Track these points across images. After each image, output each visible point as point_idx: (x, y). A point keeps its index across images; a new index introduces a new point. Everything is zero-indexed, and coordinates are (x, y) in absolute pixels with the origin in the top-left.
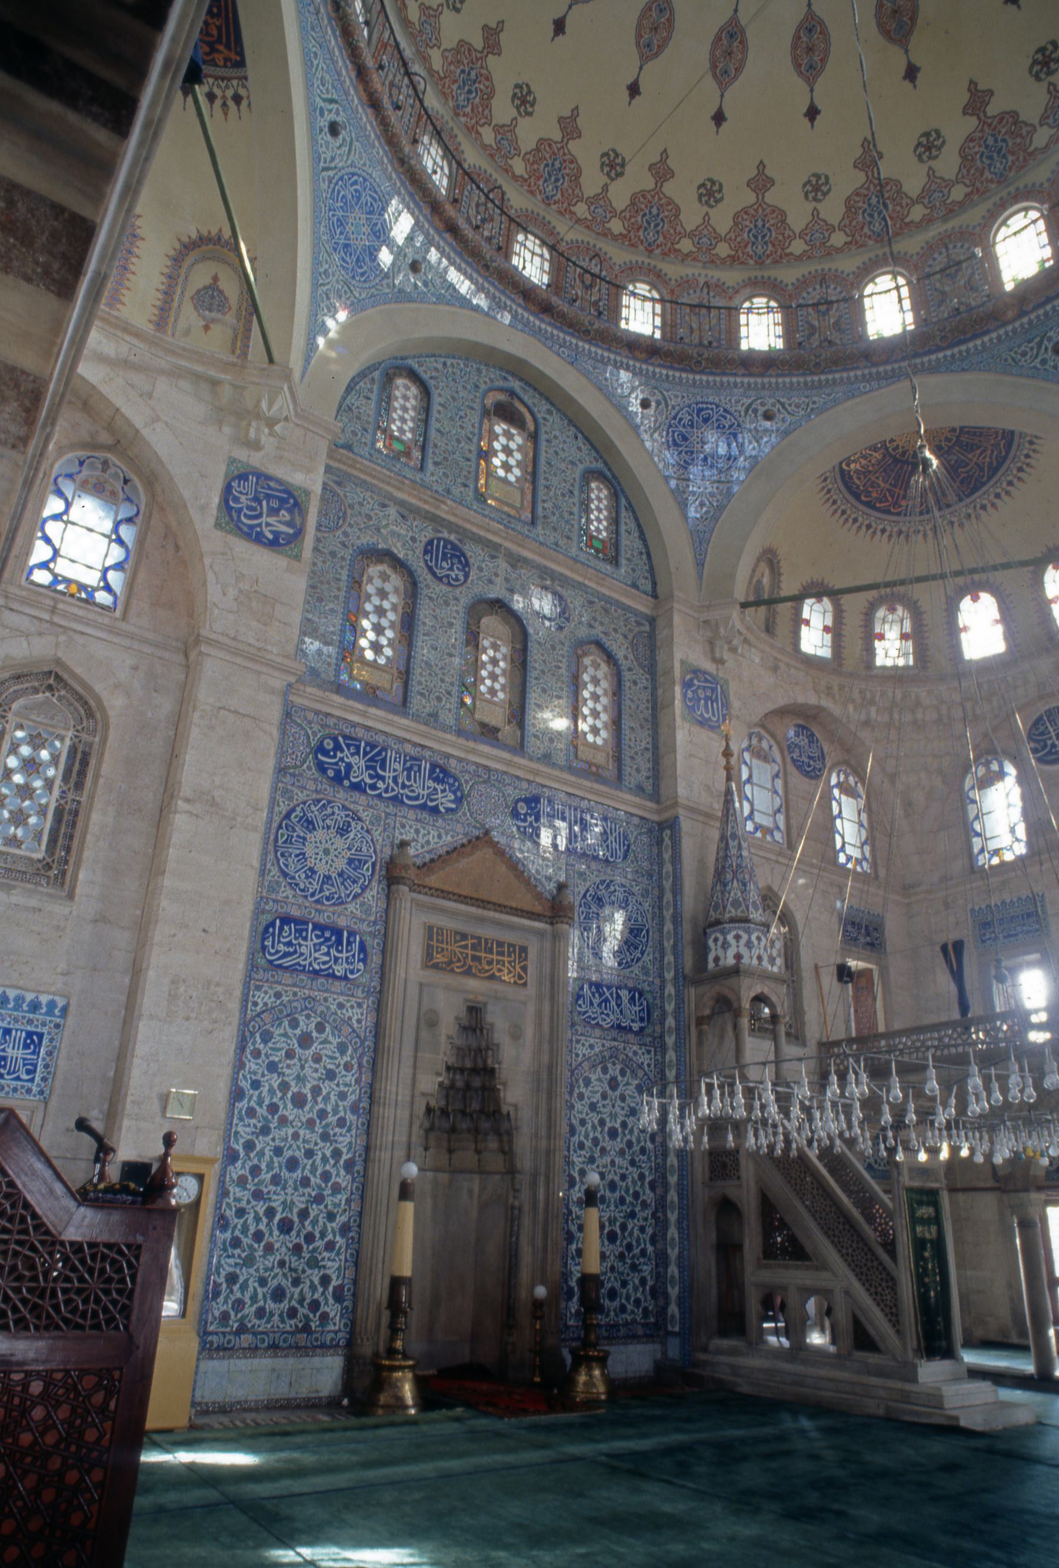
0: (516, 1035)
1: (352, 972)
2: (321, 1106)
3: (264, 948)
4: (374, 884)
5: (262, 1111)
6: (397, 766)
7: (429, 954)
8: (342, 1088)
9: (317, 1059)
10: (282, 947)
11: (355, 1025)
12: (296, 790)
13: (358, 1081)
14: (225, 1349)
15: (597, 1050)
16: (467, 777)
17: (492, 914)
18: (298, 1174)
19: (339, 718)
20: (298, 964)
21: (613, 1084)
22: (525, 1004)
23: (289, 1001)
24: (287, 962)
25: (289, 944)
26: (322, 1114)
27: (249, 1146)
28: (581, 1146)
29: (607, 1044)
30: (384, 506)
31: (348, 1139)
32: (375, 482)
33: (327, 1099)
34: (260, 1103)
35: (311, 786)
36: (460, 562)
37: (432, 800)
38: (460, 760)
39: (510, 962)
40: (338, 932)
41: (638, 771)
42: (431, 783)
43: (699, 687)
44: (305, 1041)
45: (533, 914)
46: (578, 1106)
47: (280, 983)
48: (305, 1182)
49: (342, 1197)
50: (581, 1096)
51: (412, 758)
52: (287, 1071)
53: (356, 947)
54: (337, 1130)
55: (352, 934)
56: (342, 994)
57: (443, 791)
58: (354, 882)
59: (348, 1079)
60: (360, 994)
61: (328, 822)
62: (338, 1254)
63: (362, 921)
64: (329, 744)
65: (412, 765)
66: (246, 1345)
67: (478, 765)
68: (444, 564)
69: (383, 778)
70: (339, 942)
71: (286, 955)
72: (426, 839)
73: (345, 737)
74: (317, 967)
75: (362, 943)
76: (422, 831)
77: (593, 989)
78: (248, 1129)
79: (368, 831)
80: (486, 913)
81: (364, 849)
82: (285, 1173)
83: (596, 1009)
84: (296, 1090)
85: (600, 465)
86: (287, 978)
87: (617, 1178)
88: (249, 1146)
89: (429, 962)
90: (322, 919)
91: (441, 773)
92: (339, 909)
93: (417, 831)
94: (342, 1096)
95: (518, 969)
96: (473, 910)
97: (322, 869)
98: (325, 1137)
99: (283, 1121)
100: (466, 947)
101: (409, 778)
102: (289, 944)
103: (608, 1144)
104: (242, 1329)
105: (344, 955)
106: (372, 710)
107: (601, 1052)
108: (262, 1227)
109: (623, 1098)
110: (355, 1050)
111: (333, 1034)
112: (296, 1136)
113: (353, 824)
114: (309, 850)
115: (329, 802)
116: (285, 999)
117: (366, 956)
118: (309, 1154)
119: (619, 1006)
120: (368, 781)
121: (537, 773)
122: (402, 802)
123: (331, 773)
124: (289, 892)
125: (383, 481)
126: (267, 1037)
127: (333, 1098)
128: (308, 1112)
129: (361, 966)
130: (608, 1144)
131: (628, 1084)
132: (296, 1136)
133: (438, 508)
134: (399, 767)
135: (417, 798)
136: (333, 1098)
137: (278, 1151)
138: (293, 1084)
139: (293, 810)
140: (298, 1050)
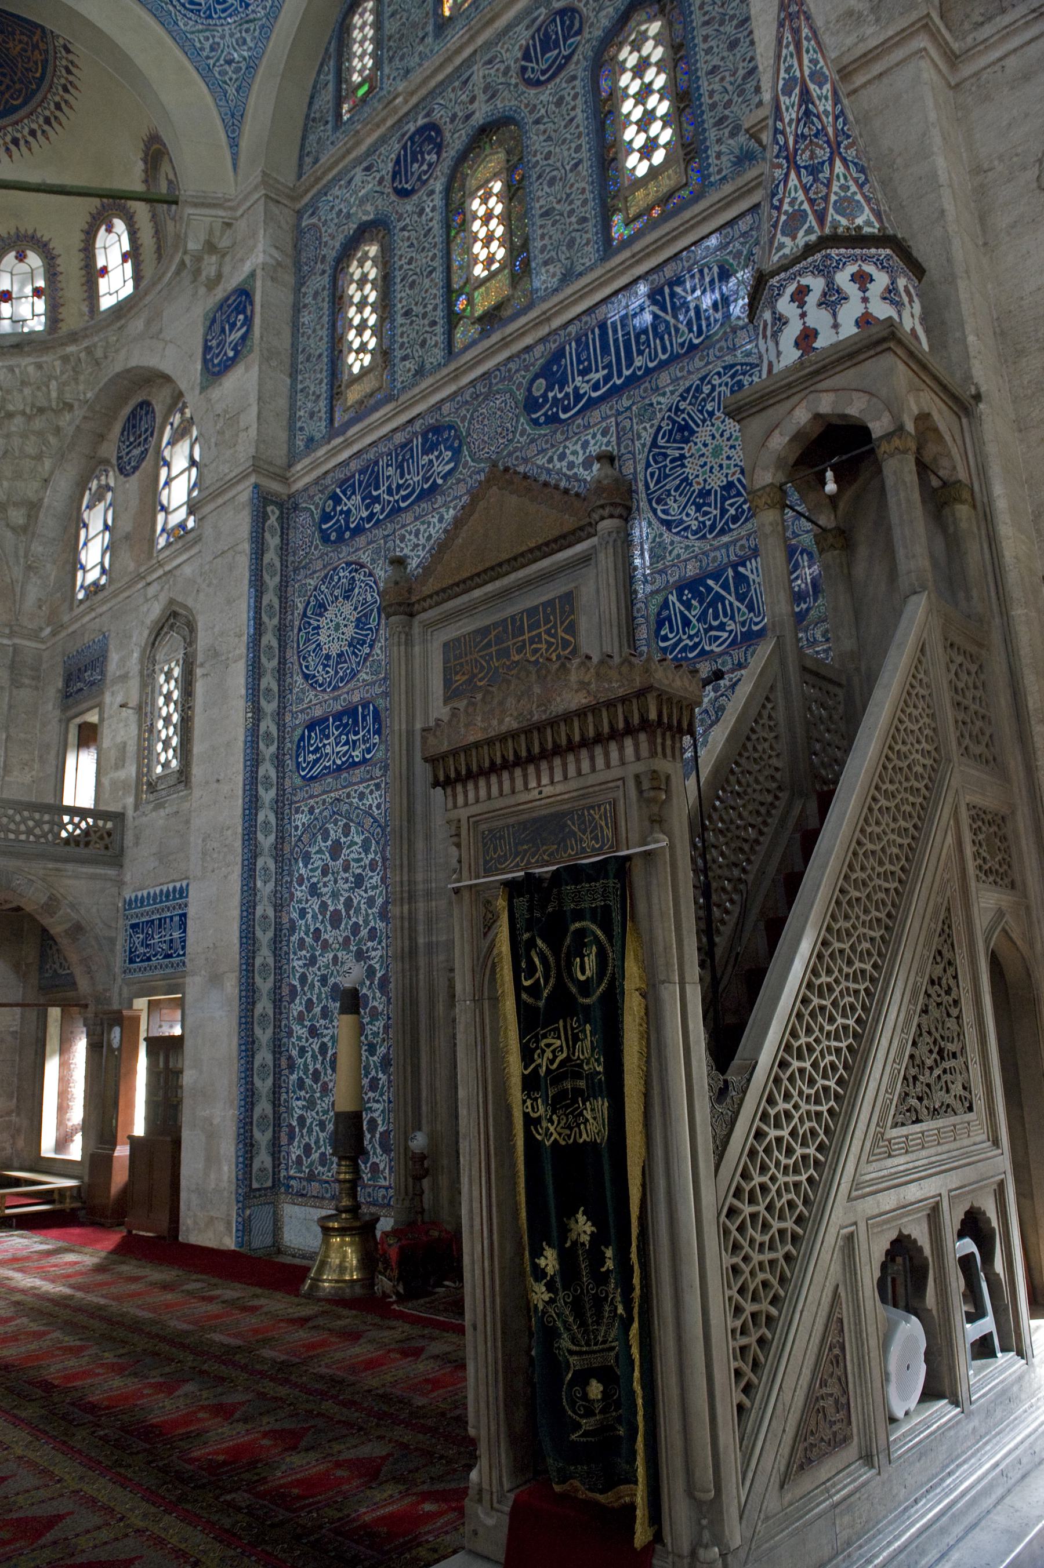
1: (369, 751)
2: (354, 919)
3: (298, 764)
5: (309, 940)
6: (391, 471)
7: (447, 682)
8: (371, 893)
9: (346, 868)
10: (311, 757)
12: (308, 581)
13: (383, 880)
14: (302, 1195)
20: (325, 768)
23: (321, 813)
24: (315, 772)
25: (317, 749)
26: (356, 929)
27: (303, 978)
31: (379, 953)
33: (358, 910)
36: (430, 139)
37: (427, 480)
39: (548, 632)
40: (351, 712)
44: (336, 850)
45: (564, 537)
47: (311, 797)
49: (380, 1024)
51: (403, 446)
52: (324, 890)
53: (370, 719)
54: (369, 944)
56: (361, 782)
57: (437, 458)
60: (378, 773)
62: (381, 1095)
63: (374, 683)
66: (315, 1194)
67: (473, 383)
68: (416, 166)
70: (356, 723)
72: (419, 536)
74: (339, 762)
75: (376, 712)
76: (422, 528)
78: (300, 963)
79: (371, 575)
80: (506, 581)
81: (369, 598)
83: (698, 626)
84: (331, 908)
86: (316, 788)
88: (303, 978)
92: (350, 686)
94: (371, 902)
95: (561, 633)
96: (489, 588)
99: (326, 946)
100: (489, 645)
101: (402, 476)
104: (311, 1177)
108: (318, 1066)
110: (378, 843)
111: (358, 833)
112: (335, 958)
113: (357, 576)
114: (322, 638)
115: (334, 569)
116: (317, 811)
117: (380, 724)
119: (741, 598)
125: (344, 157)
126: (307, 858)
129: (376, 739)
133: (395, 110)
134: (391, 471)
136: (363, 907)
137: (324, 980)
138: (329, 902)
140: (331, 863)
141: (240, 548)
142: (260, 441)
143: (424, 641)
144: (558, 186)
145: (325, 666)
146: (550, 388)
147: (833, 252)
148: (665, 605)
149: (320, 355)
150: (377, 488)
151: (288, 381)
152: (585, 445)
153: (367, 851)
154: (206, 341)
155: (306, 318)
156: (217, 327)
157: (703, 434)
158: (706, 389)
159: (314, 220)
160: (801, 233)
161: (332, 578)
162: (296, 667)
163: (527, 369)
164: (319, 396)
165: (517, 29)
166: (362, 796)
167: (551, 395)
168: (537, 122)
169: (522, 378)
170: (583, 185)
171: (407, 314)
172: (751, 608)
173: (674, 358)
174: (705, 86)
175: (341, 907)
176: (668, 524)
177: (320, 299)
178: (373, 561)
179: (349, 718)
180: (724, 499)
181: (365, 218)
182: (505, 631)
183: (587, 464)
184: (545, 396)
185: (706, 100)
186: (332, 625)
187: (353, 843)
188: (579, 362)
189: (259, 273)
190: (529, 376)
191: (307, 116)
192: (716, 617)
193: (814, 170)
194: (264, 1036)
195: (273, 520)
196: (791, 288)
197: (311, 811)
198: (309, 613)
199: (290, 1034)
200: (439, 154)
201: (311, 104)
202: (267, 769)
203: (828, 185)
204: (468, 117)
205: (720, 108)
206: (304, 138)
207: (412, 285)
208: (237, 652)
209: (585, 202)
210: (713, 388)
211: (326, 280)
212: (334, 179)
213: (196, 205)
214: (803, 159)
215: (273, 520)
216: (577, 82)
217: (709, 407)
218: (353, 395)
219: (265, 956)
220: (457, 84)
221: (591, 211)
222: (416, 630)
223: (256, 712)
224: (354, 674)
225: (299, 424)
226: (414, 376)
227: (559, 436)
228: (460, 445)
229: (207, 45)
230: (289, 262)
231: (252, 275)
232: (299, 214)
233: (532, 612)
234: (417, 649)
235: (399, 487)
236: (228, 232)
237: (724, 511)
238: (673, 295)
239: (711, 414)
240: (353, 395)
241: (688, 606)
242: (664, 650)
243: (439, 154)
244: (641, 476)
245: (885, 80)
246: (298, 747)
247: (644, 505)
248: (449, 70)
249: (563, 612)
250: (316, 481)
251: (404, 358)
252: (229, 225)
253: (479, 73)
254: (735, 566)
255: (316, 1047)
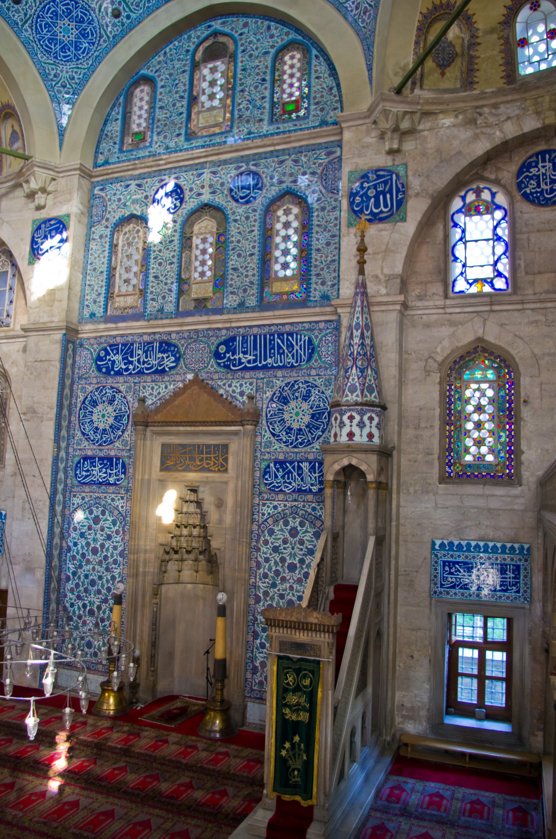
0: (220, 504)
1: (118, 480)
3: (76, 475)
4: (129, 427)
5: (78, 557)
6: (140, 352)
7: (162, 463)
9: (102, 529)
10: (84, 473)
11: (120, 509)
15: (280, 509)
16: (183, 342)
17: (201, 428)
18: (95, 588)
19: (107, 336)
21: (294, 532)
22: (226, 483)
24: (87, 480)
25: (88, 471)
28: (265, 576)
29: (289, 504)
30: (128, 186)
31: (118, 571)
32: (122, 174)
33: (107, 550)
34: (78, 553)
35: (94, 381)
37: (161, 366)
38: (178, 332)
39: (215, 458)
40: (110, 459)
41: (323, 283)
42: (160, 355)
43: (369, 188)
46: (263, 549)
47: (83, 492)
48: (99, 592)
50: (266, 542)
51: (149, 343)
53: (120, 466)
55: (118, 459)
56: (113, 493)
57: (167, 357)
58: (119, 429)
59: (117, 539)
61: (104, 399)
64: (103, 354)
65: (148, 347)
67: (189, 331)
69: (131, 363)
70: (112, 465)
71: (87, 476)
72: (156, 391)
73: (111, 346)
75: (123, 462)
76: (156, 387)
77: (278, 466)
79: (125, 398)
82: (90, 587)
83: (280, 479)
85: (293, 36)
86: (87, 489)
87: (293, 599)
89: (164, 468)
90: (102, 454)
91: (166, 346)
92: (110, 446)
93: (153, 388)
94: (115, 548)
95: (221, 460)
96: (188, 428)
97: (101, 426)
98: (107, 569)
99: (88, 562)
100: (185, 453)
101: (147, 357)
102: (88, 471)
103: (287, 574)
105: (114, 472)
106: (121, 325)
107: (283, 511)
109: (302, 542)
112: (94, 569)
114: (95, 418)
116: (86, 500)
118: (100, 578)
119: (299, 475)
120: (124, 367)
121: (230, 321)
122: (144, 373)
123: (104, 370)
124: (86, 443)
127: (111, 549)
128: (98, 558)
129: (123, 476)
130: (287, 574)
131: (306, 531)
132: (94, 569)
134: (140, 352)
135: (152, 368)
136: (111, 549)
137: (86, 576)
139: (86, 398)
140: (93, 526)
141: (53, 363)
142: (69, 310)
143: (152, 440)
144: (242, 260)
145: (95, 433)
146: (227, 352)
147: (364, 408)
148: (268, 466)
149: (102, 272)
150: (132, 357)
151: (81, 276)
152: (241, 385)
153: (115, 525)
154: (33, 238)
155: (93, 245)
156: (42, 232)
157: (293, 404)
158: (296, 387)
159: (103, 194)
160: (355, 394)
161: (102, 390)
162: (77, 426)
163: (217, 337)
164: (100, 294)
165: (231, 166)
166: (113, 500)
167: (227, 355)
168: (235, 221)
169: (215, 341)
170: (254, 266)
171: (156, 277)
172: (302, 480)
173: (284, 367)
174: (314, 254)
175: (98, 546)
176: (274, 435)
177: (103, 240)
178: (127, 392)
179: (108, 462)
180: (297, 434)
181: (135, 212)
182: (194, 450)
183: (242, 394)
184: (225, 354)
185: (313, 260)
186: (101, 414)
187: (106, 520)
188: (243, 347)
189: (73, 218)
190: (218, 342)
191: (102, 130)
192: (288, 479)
193: (362, 371)
194: (53, 597)
195: (70, 352)
196: (348, 414)
197: (83, 498)
198: (87, 403)
199: (66, 596)
200: (181, 203)
201: (105, 124)
202: (61, 475)
203: (365, 379)
204: (199, 195)
205: (319, 269)
206: (99, 142)
207: (160, 264)
208: (49, 416)
209: (254, 275)
210: (299, 388)
211: (108, 232)
212: (117, 178)
213: (39, 167)
214: (359, 363)
215: (70, 352)
216: (257, 214)
217: (296, 394)
218: (120, 302)
219: (55, 562)
220: (195, 172)
221: (256, 279)
222: (148, 434)
223: (59, 448)
224: (112, 442)
225: (86, 303)
226: (157, 311)
227: (229, 376)
228: (180, 357)
229: (53, 73)
230: (85, 211)
231: (68, 216)
232: (94, 185)
233: (208, 446)
234: (148, 442)
235: (144, 362)
236: (53, 182)
237: (297, 439)
238: (288, 339)
239: (297, 398)
240: (120, 302)
241: (278, 471)
242: (266, 484)
243: (181, 203)
244: (264, 410)
245: (385, 314)
246: (77, 466)
247: (264, 422)
248: (191, 162)
249: (222, 452)
250: (95, 338)
251: (153, 300)
252: (54, 179)
253: (207, 176)
254: (298, 462)
255: (81, 605)
